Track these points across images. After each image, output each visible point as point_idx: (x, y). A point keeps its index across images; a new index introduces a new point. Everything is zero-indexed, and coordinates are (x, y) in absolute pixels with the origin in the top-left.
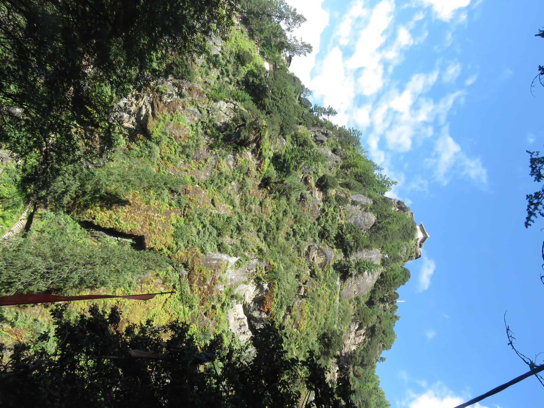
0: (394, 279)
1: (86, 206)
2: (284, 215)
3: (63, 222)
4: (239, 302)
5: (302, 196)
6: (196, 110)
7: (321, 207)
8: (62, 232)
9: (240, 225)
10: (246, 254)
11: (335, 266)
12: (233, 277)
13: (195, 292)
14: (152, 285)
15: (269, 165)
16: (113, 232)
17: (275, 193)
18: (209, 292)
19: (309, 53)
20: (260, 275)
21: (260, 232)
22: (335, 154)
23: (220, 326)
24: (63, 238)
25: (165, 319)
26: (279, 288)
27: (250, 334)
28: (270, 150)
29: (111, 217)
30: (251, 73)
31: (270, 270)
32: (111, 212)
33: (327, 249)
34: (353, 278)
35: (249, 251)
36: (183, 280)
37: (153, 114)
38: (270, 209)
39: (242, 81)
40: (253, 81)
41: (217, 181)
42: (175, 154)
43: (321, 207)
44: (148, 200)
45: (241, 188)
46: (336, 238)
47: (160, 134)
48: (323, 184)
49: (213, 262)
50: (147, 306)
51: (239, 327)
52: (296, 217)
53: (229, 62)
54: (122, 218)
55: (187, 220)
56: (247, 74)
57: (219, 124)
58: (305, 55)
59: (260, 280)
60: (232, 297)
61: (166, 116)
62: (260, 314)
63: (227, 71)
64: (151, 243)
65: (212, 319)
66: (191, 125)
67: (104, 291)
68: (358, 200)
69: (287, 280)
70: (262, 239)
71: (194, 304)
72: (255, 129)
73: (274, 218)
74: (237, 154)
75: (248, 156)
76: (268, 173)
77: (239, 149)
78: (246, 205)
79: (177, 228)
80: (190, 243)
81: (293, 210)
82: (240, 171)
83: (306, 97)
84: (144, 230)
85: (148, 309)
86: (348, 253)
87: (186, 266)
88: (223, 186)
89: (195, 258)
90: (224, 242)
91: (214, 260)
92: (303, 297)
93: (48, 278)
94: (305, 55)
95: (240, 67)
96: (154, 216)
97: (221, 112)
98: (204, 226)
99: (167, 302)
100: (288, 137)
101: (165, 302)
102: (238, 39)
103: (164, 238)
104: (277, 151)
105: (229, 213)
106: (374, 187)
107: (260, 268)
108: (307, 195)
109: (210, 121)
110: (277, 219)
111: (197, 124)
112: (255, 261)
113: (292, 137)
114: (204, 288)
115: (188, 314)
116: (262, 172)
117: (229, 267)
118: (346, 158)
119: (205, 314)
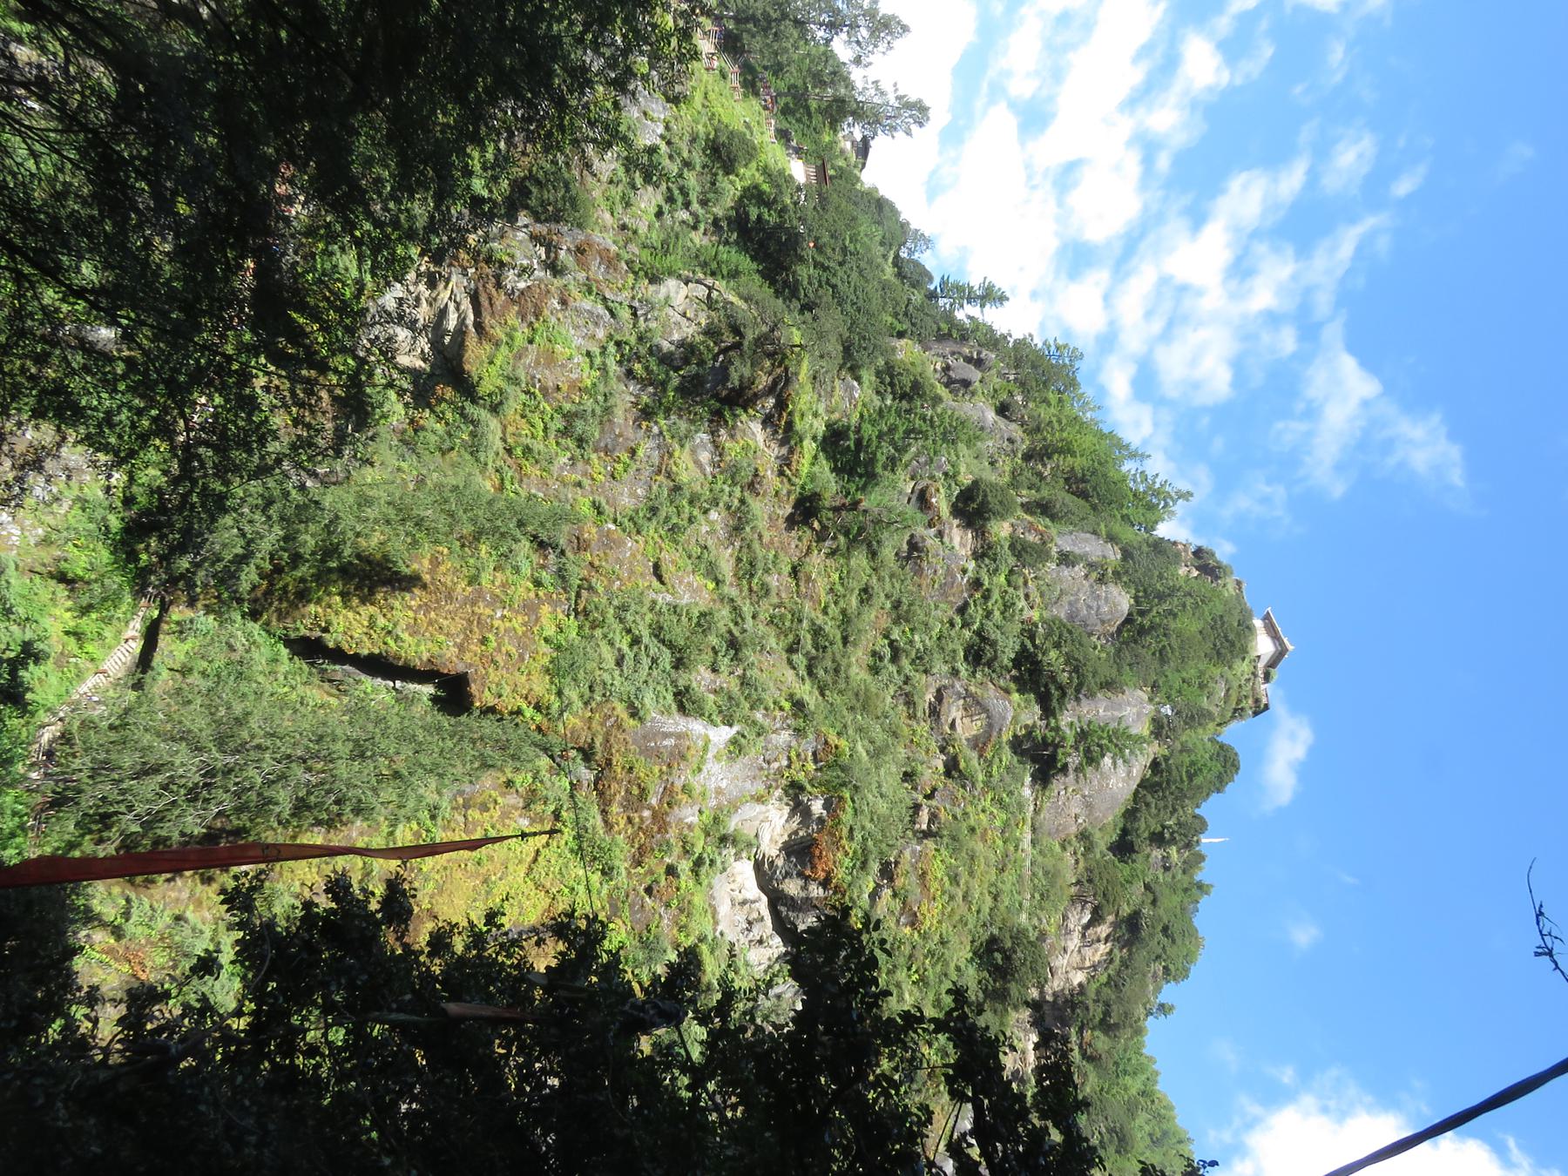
0: (1191, 777)
1: (303, 596)
2: (862, 602)
3: (240, 641)
4: (744, 855)
5: (914, 546)
6: (600, 309)
7: (970, 574)
9: (737, 634)
10: (759, 716)
11: (1016, 745)
12: (723, 784)
15: (815, 457)
16: (379, 666)
17: (835, 538)
19: (921, 125)
20: (801, 777)
22: (1005, 417)
23: (693, 925)
24: (244, 687)
25: (534, 906)
27: (777, 946)
28: (816, 415)
30: (753, 194)
31: (828, 758)
32: (372, 609)
33: (991, 694)
34: (1072, 776)
35: (766, 709)
36: (581, 795)
37: (479, 326)
38: (821, 586)
39: (728, 219)
40: (759, 217)
41: (667, 508)
42: (546, 437)
43: (970, 574)
44: (473, 571)
45: (738, 529)
46: (1017, 663)
47: (500, 382)
48: (973, 508)
50: (483, 870)
51: (745, 925)
52: (897, 605)
53: (687, 164)
54: (403, 626)
55: (588, 625)
56: (741, 198)
57: (666, 346)
58: (908, 133)
59: (802, 788)
60: (723, 839)
61: (515, 329)
62: (804, 888)
63: (684, 191)
65: (668, 905)
66: (588, 354)
67: (361, 834)
68: (1077, 551)
69: (879, 786)
70: (803, 672)
71: (617, 863)
72: (770, 355)
73: (833, 610)
74: (722, 431)
75: (753, 432)
76: (812, 480)
77: (727, 414)
78: (752, 576)
79: (558, 648)
80: (599, 690)
81: (888, 586)
82: (733, 478)
83: (916, 256)
84: (468, 657)
85: (485, 881)
86: (1055, 703)
87: (587, 754)
88: (685, 523)
89: (614, 731)
90: (694, 685)
91: (666, 735)
92: (927, 834)
93: (206, 801)
94: (908, 133)
95: (720, 177)
96: (492, 617)
97: (671, 312)
98: (636, 641)
100: (868, 376)
101: (535, 860)
102: (712, 96)
103: (524, 678)
104: (836, 416)
105: (704, 602)
106: (1125, 511)
107: (798, 755)
108: (929, 542)
109: (640, 339)
110: (844, 612)
111: (604, 348)
112: (785, 737)
113: (878, 374)
114: (641, 818)
115: (599, 893)
116: (797, 480)
117: (710, 755)
118: (1038, 429)
119: (649, 890)
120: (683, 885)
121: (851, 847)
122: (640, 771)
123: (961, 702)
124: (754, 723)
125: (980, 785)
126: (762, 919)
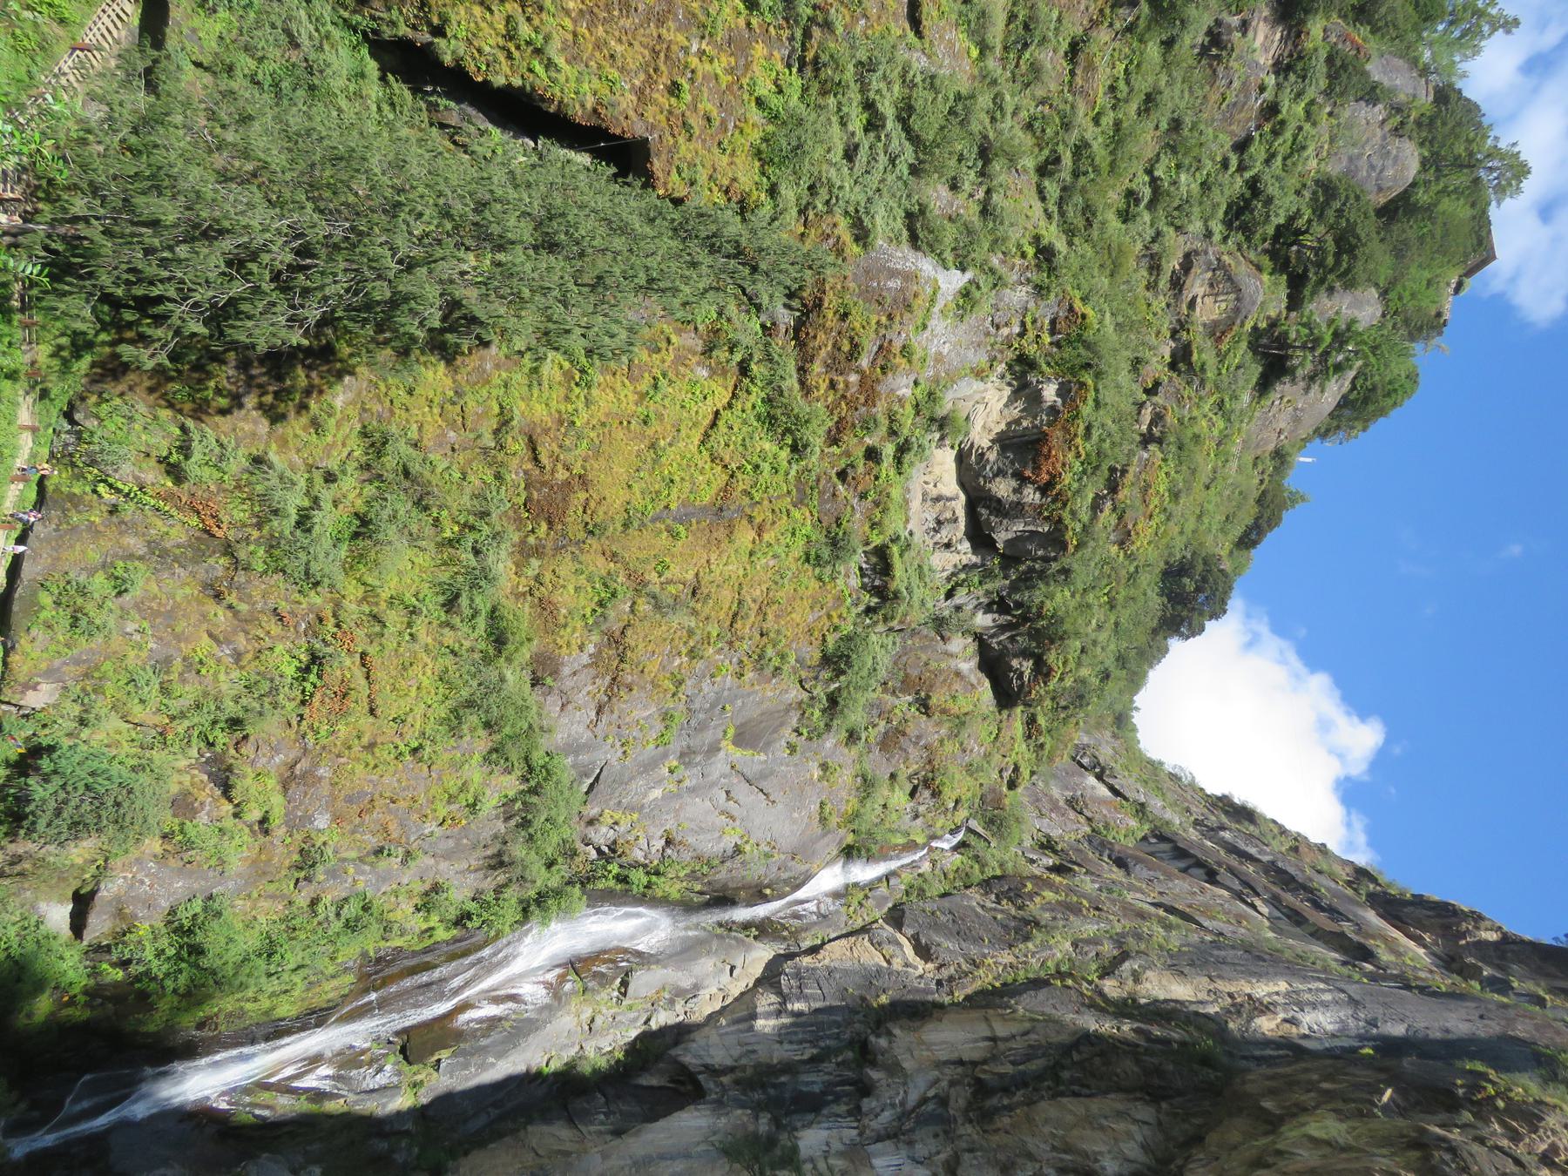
4: (947, 442)
8: (310, 80)
9: (991, 135)
10: (995, 261)
12: (945, 351)
16: (522, 112)
18: (862, 400)
20: (1031, 350)
21: (1051, 174)
23: (886, 522)
25: (709, 483)
26: (1096, 401)
29: (510, 35)
31: (1070, 330)
49: (891, 284)
55: (815, 86)
62: (1015, 491)
64: (674, 176)
65: (863, 496)
67: (497, 366)
68: (1386, 83)
70: (1053, 208)
73: (1108, 120)
78: (1026, 45)
79: (774, 118)
80: (823, 193)
85: (653, 446)
86: (1307, 292)
92: (1147, 440)
93: (306, 292)
98: (874, 124)
99: (721, 423)
101: (714, 425)
103: (725, 159)
107: (1034, 321)
110: (1117, 125)
112: (1019, 295)
114: (847, 385)
117: (936, 310)
119: (842, 475)
121: (1084, 447)
122: (856, 321)
123: (1209, 274)
125: (1208, 386)
126: (956, 520)
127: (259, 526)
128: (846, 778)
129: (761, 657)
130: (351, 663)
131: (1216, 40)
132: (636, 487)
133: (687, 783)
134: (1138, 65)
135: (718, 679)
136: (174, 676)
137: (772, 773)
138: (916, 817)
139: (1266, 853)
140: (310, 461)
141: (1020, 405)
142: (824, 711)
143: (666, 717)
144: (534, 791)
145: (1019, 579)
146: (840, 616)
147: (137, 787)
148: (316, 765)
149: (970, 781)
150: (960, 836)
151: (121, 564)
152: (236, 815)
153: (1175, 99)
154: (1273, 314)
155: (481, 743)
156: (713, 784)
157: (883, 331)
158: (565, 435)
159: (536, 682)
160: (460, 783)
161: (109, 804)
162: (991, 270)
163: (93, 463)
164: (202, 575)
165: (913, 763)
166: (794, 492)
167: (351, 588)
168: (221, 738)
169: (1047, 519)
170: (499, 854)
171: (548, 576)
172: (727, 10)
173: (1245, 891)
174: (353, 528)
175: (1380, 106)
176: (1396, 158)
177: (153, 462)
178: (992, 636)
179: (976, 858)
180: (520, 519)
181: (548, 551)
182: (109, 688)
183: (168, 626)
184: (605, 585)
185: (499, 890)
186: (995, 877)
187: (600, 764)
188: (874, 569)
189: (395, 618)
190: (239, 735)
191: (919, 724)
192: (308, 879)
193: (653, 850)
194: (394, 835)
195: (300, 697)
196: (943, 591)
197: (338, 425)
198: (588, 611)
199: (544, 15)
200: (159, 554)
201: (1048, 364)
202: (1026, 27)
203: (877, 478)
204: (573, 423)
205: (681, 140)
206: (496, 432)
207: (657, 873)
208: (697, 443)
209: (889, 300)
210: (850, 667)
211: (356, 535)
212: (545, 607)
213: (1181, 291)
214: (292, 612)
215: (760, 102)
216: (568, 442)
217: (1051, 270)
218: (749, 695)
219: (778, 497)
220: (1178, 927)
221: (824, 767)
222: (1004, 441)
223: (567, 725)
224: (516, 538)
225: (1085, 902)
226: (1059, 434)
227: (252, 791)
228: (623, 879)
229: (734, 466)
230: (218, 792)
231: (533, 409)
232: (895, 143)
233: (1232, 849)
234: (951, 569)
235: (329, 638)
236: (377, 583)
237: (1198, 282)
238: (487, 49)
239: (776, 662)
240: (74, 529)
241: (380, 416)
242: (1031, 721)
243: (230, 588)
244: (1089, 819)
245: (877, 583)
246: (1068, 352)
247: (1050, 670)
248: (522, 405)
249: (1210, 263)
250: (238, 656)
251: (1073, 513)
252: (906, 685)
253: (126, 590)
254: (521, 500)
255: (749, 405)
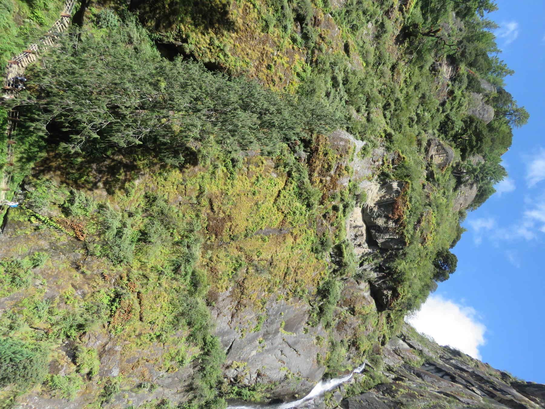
3: (135, 35)
4: (359, 204)
10: (372, 138)
12: (359, 169)
13: (315, 184)
14: (263, 169)
18: (332, 187)
20: (386, 170)
25: (277, 219)
29: (211, 44)
31: (399, 163)
43: (450, 87)
62: (385, 223)
65: (332, 225)
67: (200, 170)
78: (380, 64)
79: (303, 80)
85: (256, 204)
86: (467, 155)
98: (335, 84)
99: (281, 195)
101: (278, 196)
107: (387, 160)
110: (407, 92)
112: (380, 151)
116: (405, 13)
117: (355, 154)
120: (339, 216)
124: (372, 142)
125: (441, 186)
126: (362, 235)
127: (99, 236)
128: (326, 343)
129: (295, 291)
130: (133, 296)
131: (434, 69)
132: (250, 221)
133: (266, 348)
134: (413, 74)
135: (279, 301)
136: (55, 305)
137: (299, 342)
138: (349, 359)
139: (470, 369)
140: (123, 208)
141: (384, 190)
142: (317, 314)
143: (259, 318)
144: (207, 354)
145: (387, 257)
146: (324, 273)
147: (34, 359)
148: (115, 345)
149: (369, 343)
150: (363, 367)
151: (37, 253)
152: (77, 371)
153: (424, 87)
154: (458, 161)
155: (185, 332)
156: (275, 348)
157: (339, 161)
158: (223, 199)
159: (208, 304)
160: (176, 352)
161: (21, 367)
162: (372, 141)
163: (30, 206)
164: (72, 258)
165: (348, 337)
166: (308, 223)
167: (135, 263)
168: (74, 333)
169: (397, 233)
170: (191, 384)
171: (215, 258)
172: (286, 42)
173: (468, 385)
174: (138, 237)
175: (481, 94)
176: (487, 111)
177: (56, 207)
178: (376, 282)
179: (371, 376)
180: (204, 234)
181: (215, 247)
182: (25, 311)
183: (54, 282)
184: (237, 261)
185: (190, 401)
186: (379, 384)
187: (232, 340)
188: (336, 254)
189: (153, 276)
190: (82, 332)
191: (351, 319)
192: (107, 402)
193: (252, 379)
194: (147, 378)
195: (110, 314)
196: (359, 263)
197: (136, 192)
198: (230, 273)
199: (224, 38)
200: (55, 248)
201: (393, 175)
202: (379, 58)
203: (337, 217)
204: (227, 194)
205: (271, 86)
206: (197, 197)
207: (254, 390)
208: (272, 203)
209: (341, 149)
210: (330, 294)
211: (139, 240)
212: (213, 270)
213: (428, 153)
214: (109, 275)
215: (298, 75)
216: (224, 202)
217: (391, 142)
218: (290, 308)
219: (302, 225)
220: (453, 402)
221: (318, 338)
222: (379, 204)
223: (219, 323)
224: (203, 240)
225: (416, 393)
226: (401, 200)
227: (86, 359)
228: (239, 394)
229: (286, 212)
230: (70, 360)
231: (212, 188)
232: (342, 93)
233: (457, 367)
234: (361, 254)
235: (124, 286)
236: (146, 261)
237: (433, 150)
238: (203, 48)
239: (301, 293)
240: (18, 237)
241: (153, 189)
242: (388, 317)
243: (83, 264)
244: (403, 358)
245: (338, 260)
246: (399, 172)
247: (399, 294)
248: (208, 186)
249: (436, 143)
250: (84, 295)
251: (407, 231)
252: (345, 303)
253: (38, 265)
254: (206, 225)
255: (291, 188)
